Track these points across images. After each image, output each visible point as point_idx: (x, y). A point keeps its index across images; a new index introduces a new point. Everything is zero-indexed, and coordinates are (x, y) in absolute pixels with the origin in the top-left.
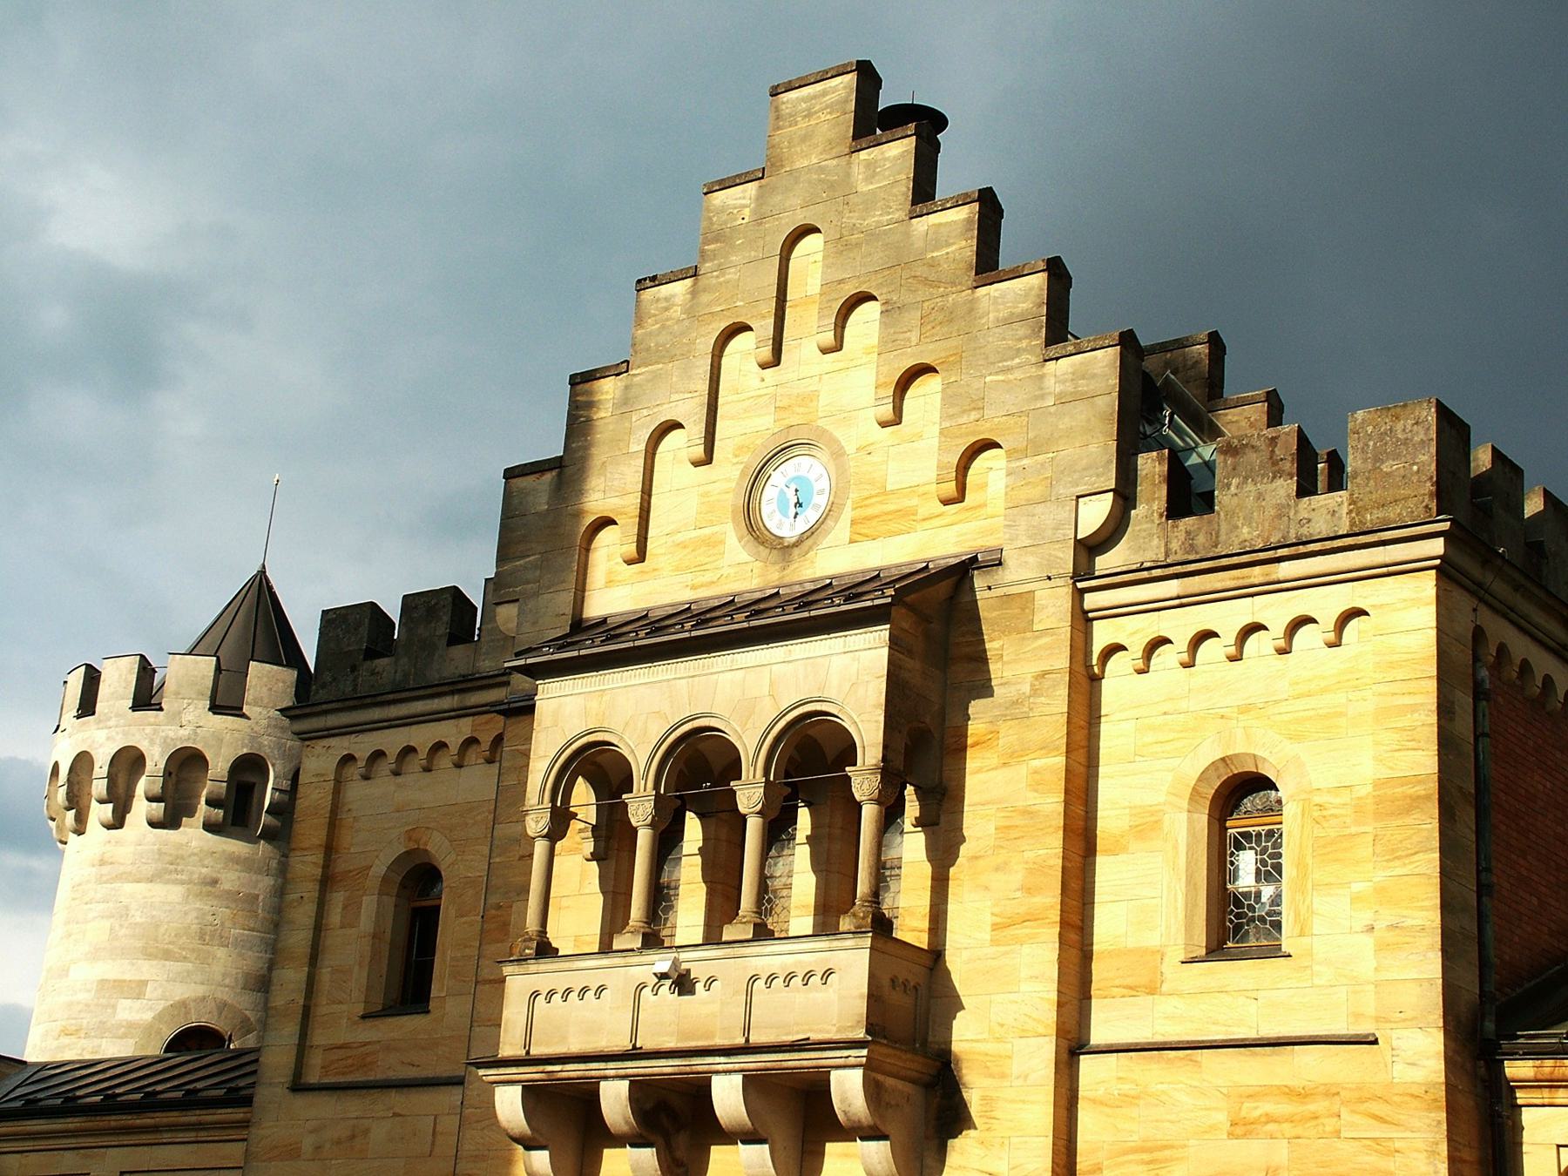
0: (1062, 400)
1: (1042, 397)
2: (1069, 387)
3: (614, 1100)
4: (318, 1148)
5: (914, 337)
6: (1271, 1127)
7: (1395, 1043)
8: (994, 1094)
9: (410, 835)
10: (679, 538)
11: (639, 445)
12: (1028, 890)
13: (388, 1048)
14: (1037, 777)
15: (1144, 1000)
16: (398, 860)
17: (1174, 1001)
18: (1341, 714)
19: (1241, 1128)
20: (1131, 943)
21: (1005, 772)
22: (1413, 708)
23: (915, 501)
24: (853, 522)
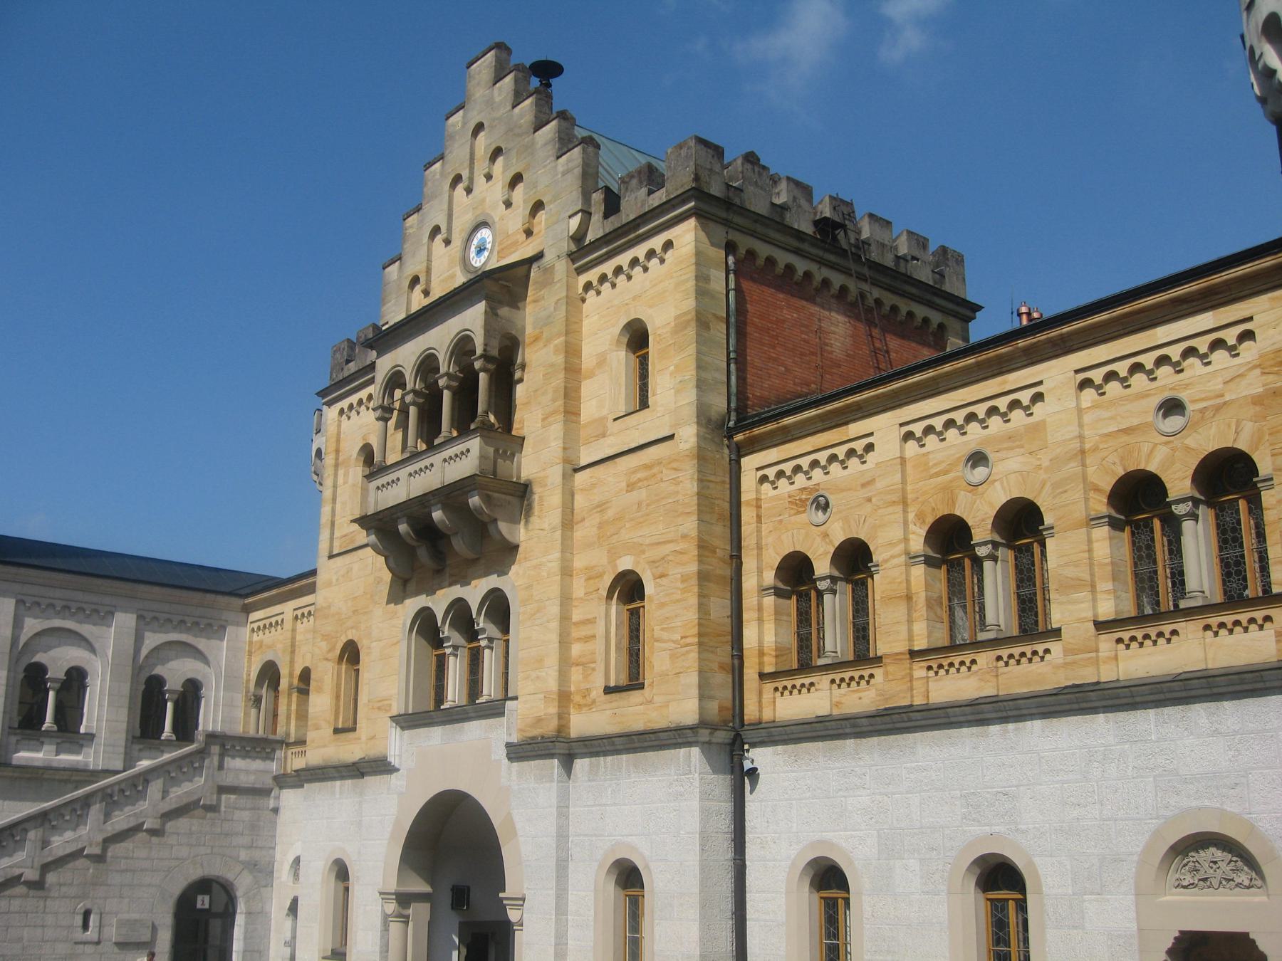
0: (564, 174)
3: (403, 528)
12: (554, 400)
15: (602, 441)
17: (612, 438)
19: (631, 487)
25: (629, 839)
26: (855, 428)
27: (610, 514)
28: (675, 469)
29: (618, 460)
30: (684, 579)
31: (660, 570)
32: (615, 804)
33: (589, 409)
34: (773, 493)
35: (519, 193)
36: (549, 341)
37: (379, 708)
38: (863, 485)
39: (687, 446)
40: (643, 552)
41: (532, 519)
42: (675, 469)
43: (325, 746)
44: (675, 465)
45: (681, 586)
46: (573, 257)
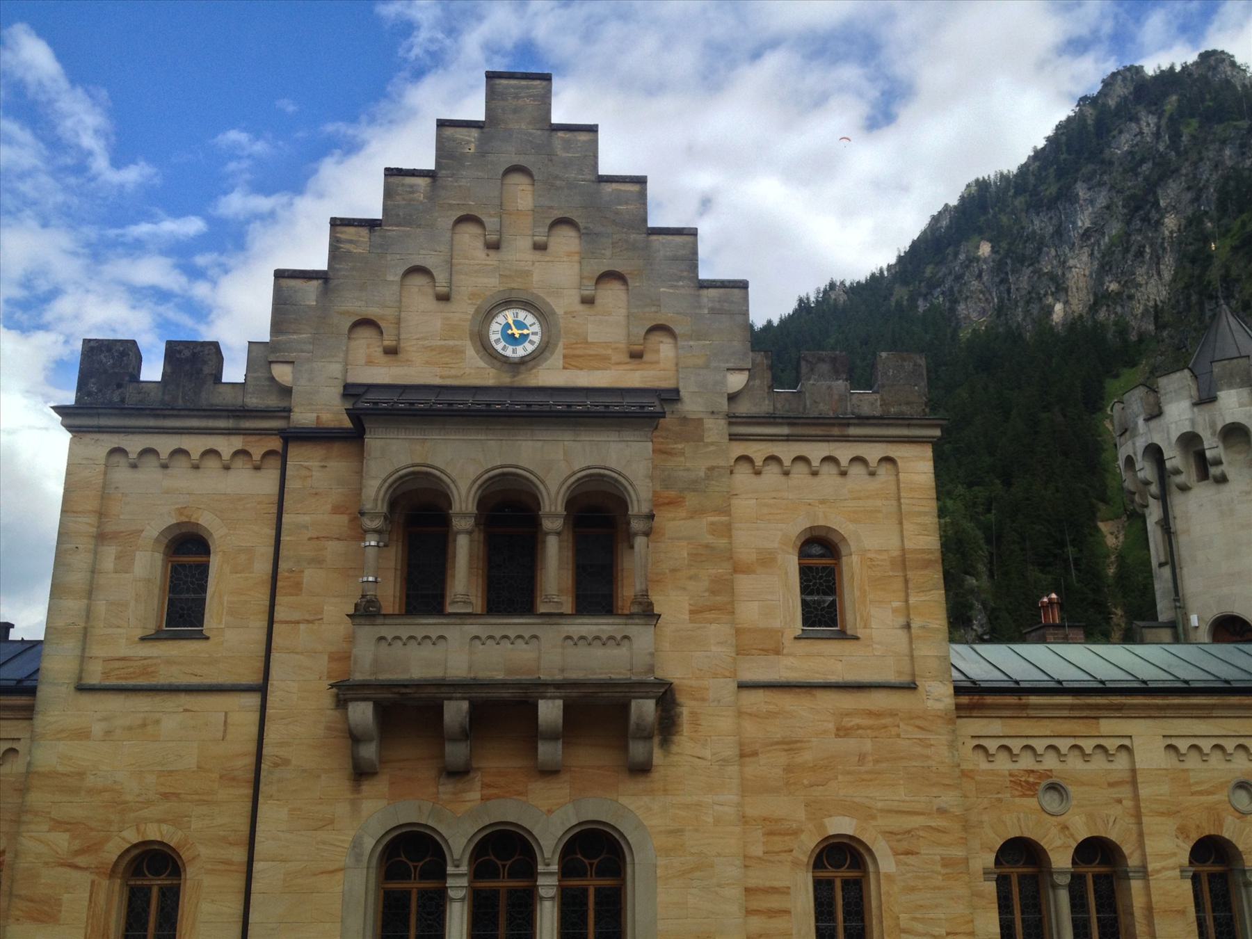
0: (713, 311)
1: (700, 307)
2: (717, 305)
4: (108, 733)
5: (608, 253)
6: (860, 731)
9: (180, 511)
10: (426, 343)
11: (394, 276)
13: (169, 662)
15: (772, 657)
16: (169, 528)
17: (791, 659)
18: (879, 511)
19: (843, 732)
22: (925, 514)
23: (610, 352)
24: (565, 357)
26: (1107, 726)
27: (807, 757)
30: (947, 862)
31: (904, 845)
33: (749, 613)
34: (984, 765)
35: (612, 296)
36: (695, 513)
38: (1111, 785)
39: (940, 706)
40: (874, 817)
41: (676, 738)
44: (918, 722)
45: (943, 871)
46: (732, 419)
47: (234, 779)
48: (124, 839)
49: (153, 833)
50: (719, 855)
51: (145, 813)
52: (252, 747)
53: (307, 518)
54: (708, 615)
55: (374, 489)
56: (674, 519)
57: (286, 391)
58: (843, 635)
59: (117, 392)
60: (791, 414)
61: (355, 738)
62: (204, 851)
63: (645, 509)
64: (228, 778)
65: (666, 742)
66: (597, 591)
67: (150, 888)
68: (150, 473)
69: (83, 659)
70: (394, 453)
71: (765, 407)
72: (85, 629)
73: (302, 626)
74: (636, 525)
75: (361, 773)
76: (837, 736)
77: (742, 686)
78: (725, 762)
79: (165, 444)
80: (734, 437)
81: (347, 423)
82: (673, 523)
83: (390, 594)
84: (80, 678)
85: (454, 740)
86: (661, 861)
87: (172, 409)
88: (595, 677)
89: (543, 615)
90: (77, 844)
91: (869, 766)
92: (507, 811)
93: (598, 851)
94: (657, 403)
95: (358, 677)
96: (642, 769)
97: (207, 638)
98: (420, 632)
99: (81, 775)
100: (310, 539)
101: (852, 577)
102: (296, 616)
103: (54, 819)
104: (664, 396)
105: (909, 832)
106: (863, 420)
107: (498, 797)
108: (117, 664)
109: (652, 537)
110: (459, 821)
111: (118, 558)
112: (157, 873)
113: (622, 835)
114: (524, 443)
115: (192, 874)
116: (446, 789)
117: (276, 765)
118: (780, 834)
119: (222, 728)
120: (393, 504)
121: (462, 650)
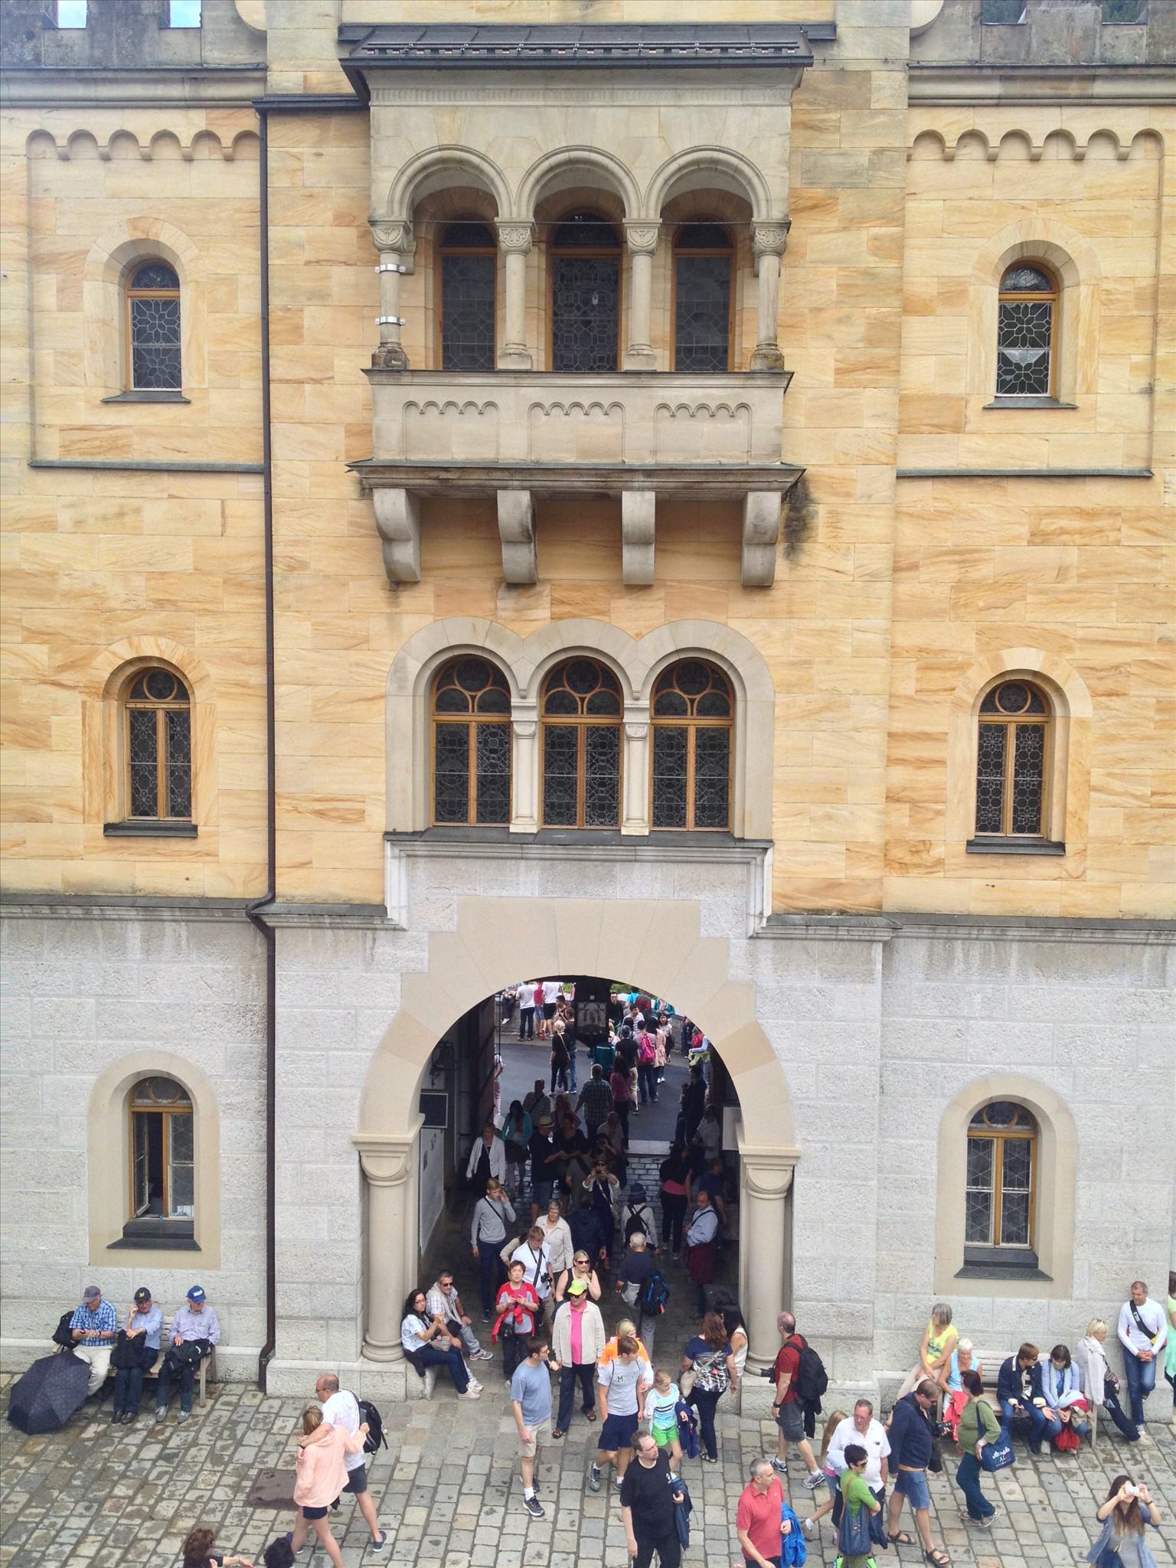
4: (79, 523)
6: (1065, 537)
7: (1168, 479)
8: (840, 510)
9: (134, 223)
13: (144, 433)
14: (878, 243)
15: (950, 437)
16: (122, 248)
18: (1127, 218)
19: (1039, 538)
20: (938, 390)
21: (844, 237)
25: (1023, 1070)
27: (985, 571)
28: (1148, 531)
29: (1012, 486)
31: (1109, 684)
32: (990, 1018)
33: (921, 373)
36: (850, 224)
37: (321, 814)
40: (1070, 649)
41: (806, 546)
42: (1148, 531)
43: (72, 858)
44: (1149, 524)
45: (1157, 718)
46: (916, 71)
47: (241, 585)
48: (114, 653)
49: (151, 648)
50: (857, 693)
51: (137, 623)
52: (260, 545)
53: (301, 233)
54: (860, 376)
55: (389, 191)
56: (820, 232)
57: (258, 39)
58: (1055, 405)
59: (30, 45)
60: (1007, 62)
61: (387, 538)
62: (212, 670)
63: (777, 214)
64: (234, 583)
65: (792, 550)
66: (704, 341)
67: (154, 712)
68: (86, 168)
69: (33, 426)
70: (415, 127)
71: (968, 52)
72: (31, 387)
73: (307, 387)
74: (764, 239)
75: (398, 582)
76: (1031, 543)
77: (902, 477)
78: (873, 577)
79: (103, 124)
80: (916, 102)
81: (347, 88)
82: (817, 238)
83: (420, 342)
84: (34, 453)
85: (512, 542)
86: (780, 699)
87: (105, 70)
88: (699, 461)
89: (626, 373)
90: (59, 659)
91: (1072, 583)
92: (585, 634)
93: (699, 683)
94: (801, 43)
95: (384, 456)
96: (760, 585)
97: (188, 402)
98: (461, 396)
99: (53, 575)
100: (308, 263)
101: (1077, 318)
102: (298, 373)
103: (25, 629)
104: (812, 35)
105: (1116, 667)
106: (1118, 70)
107: (574, 616)
108: (78, 435)
109: (786, 259)
110: (524, 643)
111: (61, 290)
112: (160, 695)
113: (731, 666)
114: (601, 110)
115: (200, 697)
116: (507, 604)
117: (292, 568)
118: (939, 669)
119: (219, 520)
120: (417, 211)
121: (522, 421)
